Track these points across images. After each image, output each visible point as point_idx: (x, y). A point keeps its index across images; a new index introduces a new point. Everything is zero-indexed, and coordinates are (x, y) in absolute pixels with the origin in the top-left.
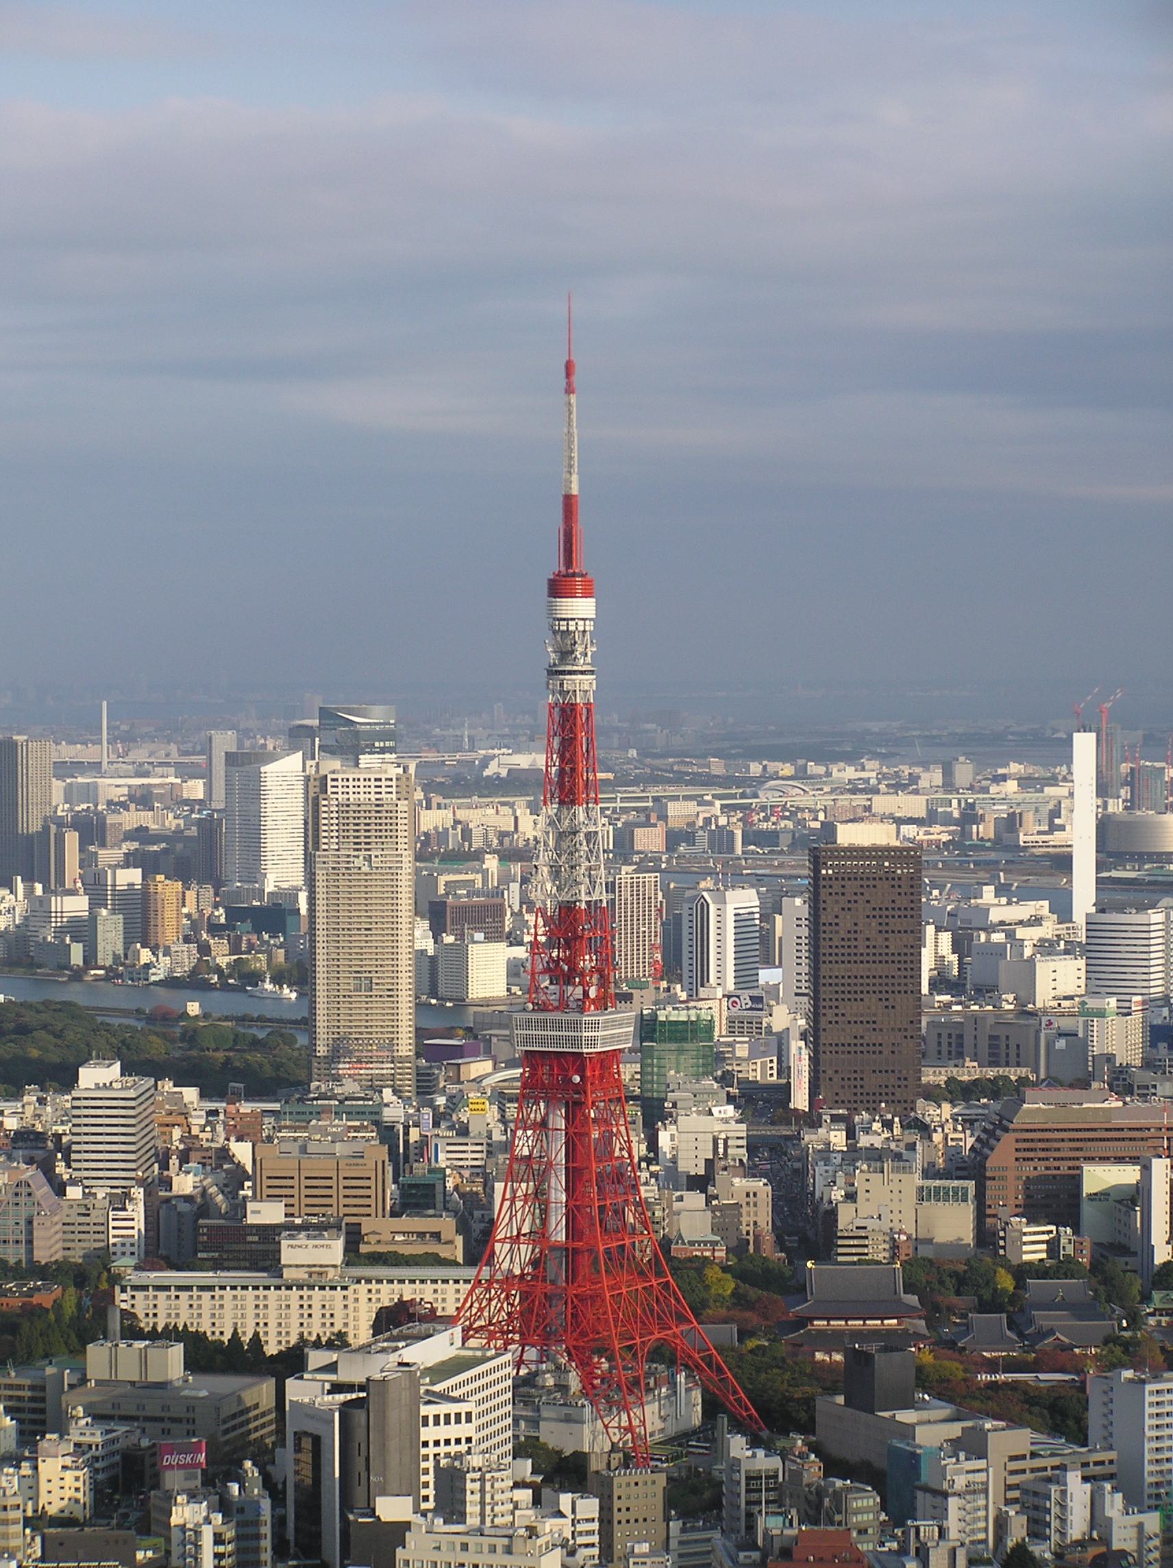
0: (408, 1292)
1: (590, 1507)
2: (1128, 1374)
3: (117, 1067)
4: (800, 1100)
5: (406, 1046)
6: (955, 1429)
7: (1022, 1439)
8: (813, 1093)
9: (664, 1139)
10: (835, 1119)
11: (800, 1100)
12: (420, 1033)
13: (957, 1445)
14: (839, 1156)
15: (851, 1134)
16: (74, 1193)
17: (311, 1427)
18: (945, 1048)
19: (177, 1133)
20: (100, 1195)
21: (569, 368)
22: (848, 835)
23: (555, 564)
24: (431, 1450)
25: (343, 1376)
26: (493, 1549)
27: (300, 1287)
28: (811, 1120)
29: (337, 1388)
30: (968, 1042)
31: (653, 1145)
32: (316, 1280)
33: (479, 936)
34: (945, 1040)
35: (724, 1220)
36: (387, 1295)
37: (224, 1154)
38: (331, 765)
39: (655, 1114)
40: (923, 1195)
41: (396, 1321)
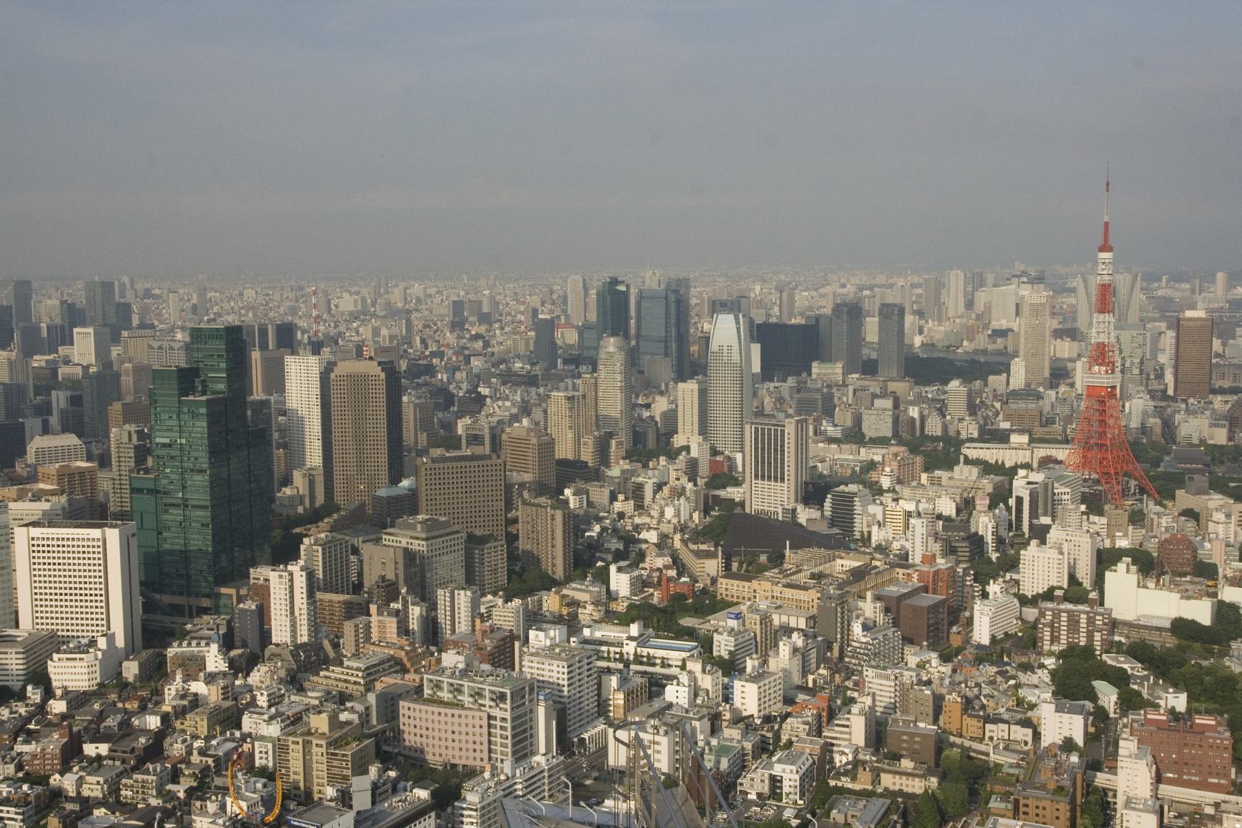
0: (1049, 452)
1: (1104, 520)
4: (1171, 392)
5: (1047, 374)
6: (1222, 502)
8: (1175, 390)
9: (1127, 405)
11: (1171, 392)
16: (948, 417)
17: (1020, 495)
21: (1108, 184)
22: (1189, 314)
23: (1100, 243)
25: (1031, 479)
28: (1174, 399)
31: (1123, 406)
32: (1020, 448)
40: (1212, 425)
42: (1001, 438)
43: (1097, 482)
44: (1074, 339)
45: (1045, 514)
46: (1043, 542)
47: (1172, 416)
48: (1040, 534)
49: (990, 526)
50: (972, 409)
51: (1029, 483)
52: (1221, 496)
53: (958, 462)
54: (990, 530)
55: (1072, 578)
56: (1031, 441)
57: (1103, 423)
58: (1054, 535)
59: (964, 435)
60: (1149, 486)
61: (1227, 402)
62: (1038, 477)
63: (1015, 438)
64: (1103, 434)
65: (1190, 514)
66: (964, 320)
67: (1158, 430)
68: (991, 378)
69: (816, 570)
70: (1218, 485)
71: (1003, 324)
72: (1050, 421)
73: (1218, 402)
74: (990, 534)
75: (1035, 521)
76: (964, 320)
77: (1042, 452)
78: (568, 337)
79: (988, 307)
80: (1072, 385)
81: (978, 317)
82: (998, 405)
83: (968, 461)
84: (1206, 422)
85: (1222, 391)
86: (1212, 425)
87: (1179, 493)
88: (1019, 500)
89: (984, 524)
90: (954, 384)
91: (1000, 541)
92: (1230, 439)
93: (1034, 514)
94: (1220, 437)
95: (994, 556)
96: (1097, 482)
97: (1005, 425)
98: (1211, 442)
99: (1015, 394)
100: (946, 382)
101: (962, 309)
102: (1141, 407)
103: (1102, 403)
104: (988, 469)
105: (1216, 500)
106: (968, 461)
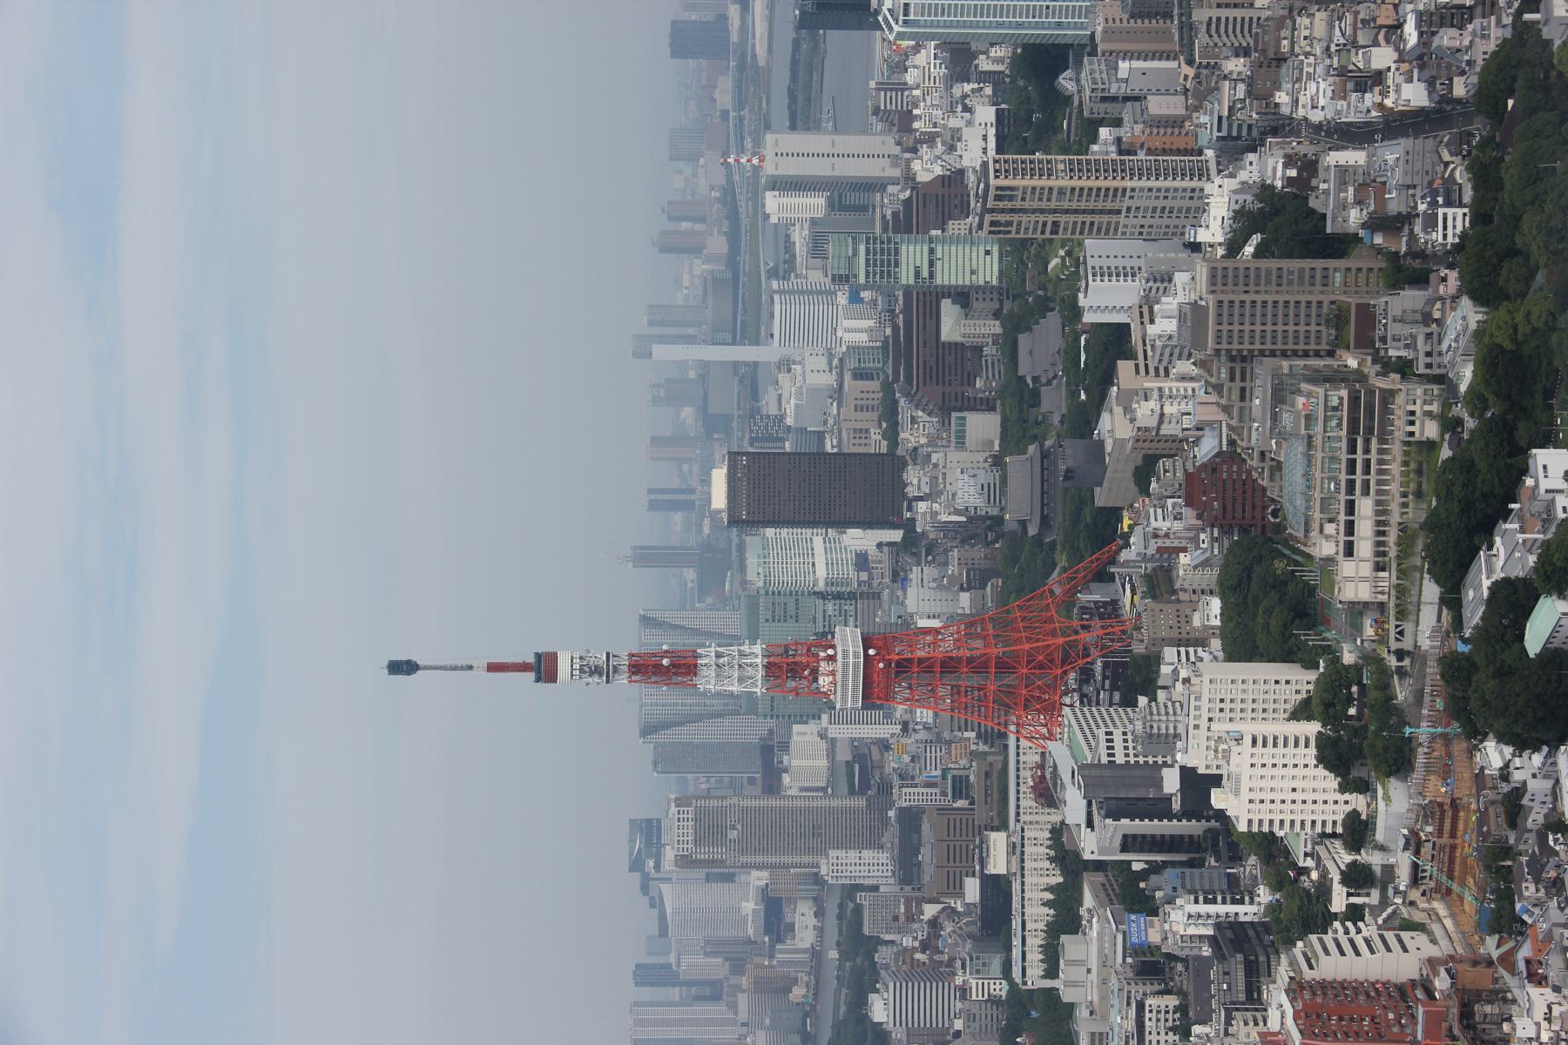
1: (1169, 653)
2: (1081, 296)
3: (872, 997)
5: (860, 802)
6: (1118, 410)
7: (1124, 368)
8: (894, 526)
10: (910, 509)
11: (896, 535)
12: (852, 792)
13: (1127, 410)
14: (935, 505)
15: (920, 499)
16: (958, 1024)
18: (863, 441)
19: (918, 956)
20: (959, 1005)
22: (719, 499)
24: (1132, 760)
25: (1082, 821)
26: (1197, 708)
27: (1023, 861)
29: (1090, 824)
30: (859, 425)
33: (785, 758)
34: (857, 441)
35: (975, 581)
36: (1028, 802)
37: (934, 923)
38: (669, 854)
39: (908, 631)
40: (961, 443)
42: (998, 891)
43: (1086, 675)
44: (785, 747)
45: (1159, 783)
46: (1216, 780)
47: (945, 527)
49: (1193, 909)
50: (939, 972)
51: (1090, 824)
52: (1105, 417)
53: (1052, 994)
54: (1203, 908)
55: (1301, 712)
56: (1003, 826)
57: (949, 665)
58: (1196, 756)
59: (1000, 989)
60: (1089, 562)
61: (914, 420)
62: (1074, 806)
63: (998, 864)
64: (978, 665)
65: (1144, 474)
66: (743, 1000)
67: (978, 553)
68: (866, 931)
70: (1083, 421)
71: (749, 906)
72: (960, 787)
73: (911, 437)
74: (1212, 909)
75: (1176, 805)
76: (743, 1000)
77: (1022, 799)
79: (713, 946)
80: (885, 745)
81: (738, 967)
82: (930, 910)
83: (1052, 972)
84: (954, 456)
85: (892, 435)
86: (961, 443)
87: (1102, 498)
88: (1129, 843)
89: (1186, 921)
90: (879, 1010)
91: (1236, 891)
92: (988, 406)
93: (1159, 808)
94: (983, 426)
95: (1264, 895)
96: (1086, 675)
97: (972, 889)
98: (997, 448)
99: (907, 869)
101: (718, 1010)
102: (926, 593)
103: (903, 667)
104: (1066, 920)
105: (1113, 426)
106: (1052, 972)
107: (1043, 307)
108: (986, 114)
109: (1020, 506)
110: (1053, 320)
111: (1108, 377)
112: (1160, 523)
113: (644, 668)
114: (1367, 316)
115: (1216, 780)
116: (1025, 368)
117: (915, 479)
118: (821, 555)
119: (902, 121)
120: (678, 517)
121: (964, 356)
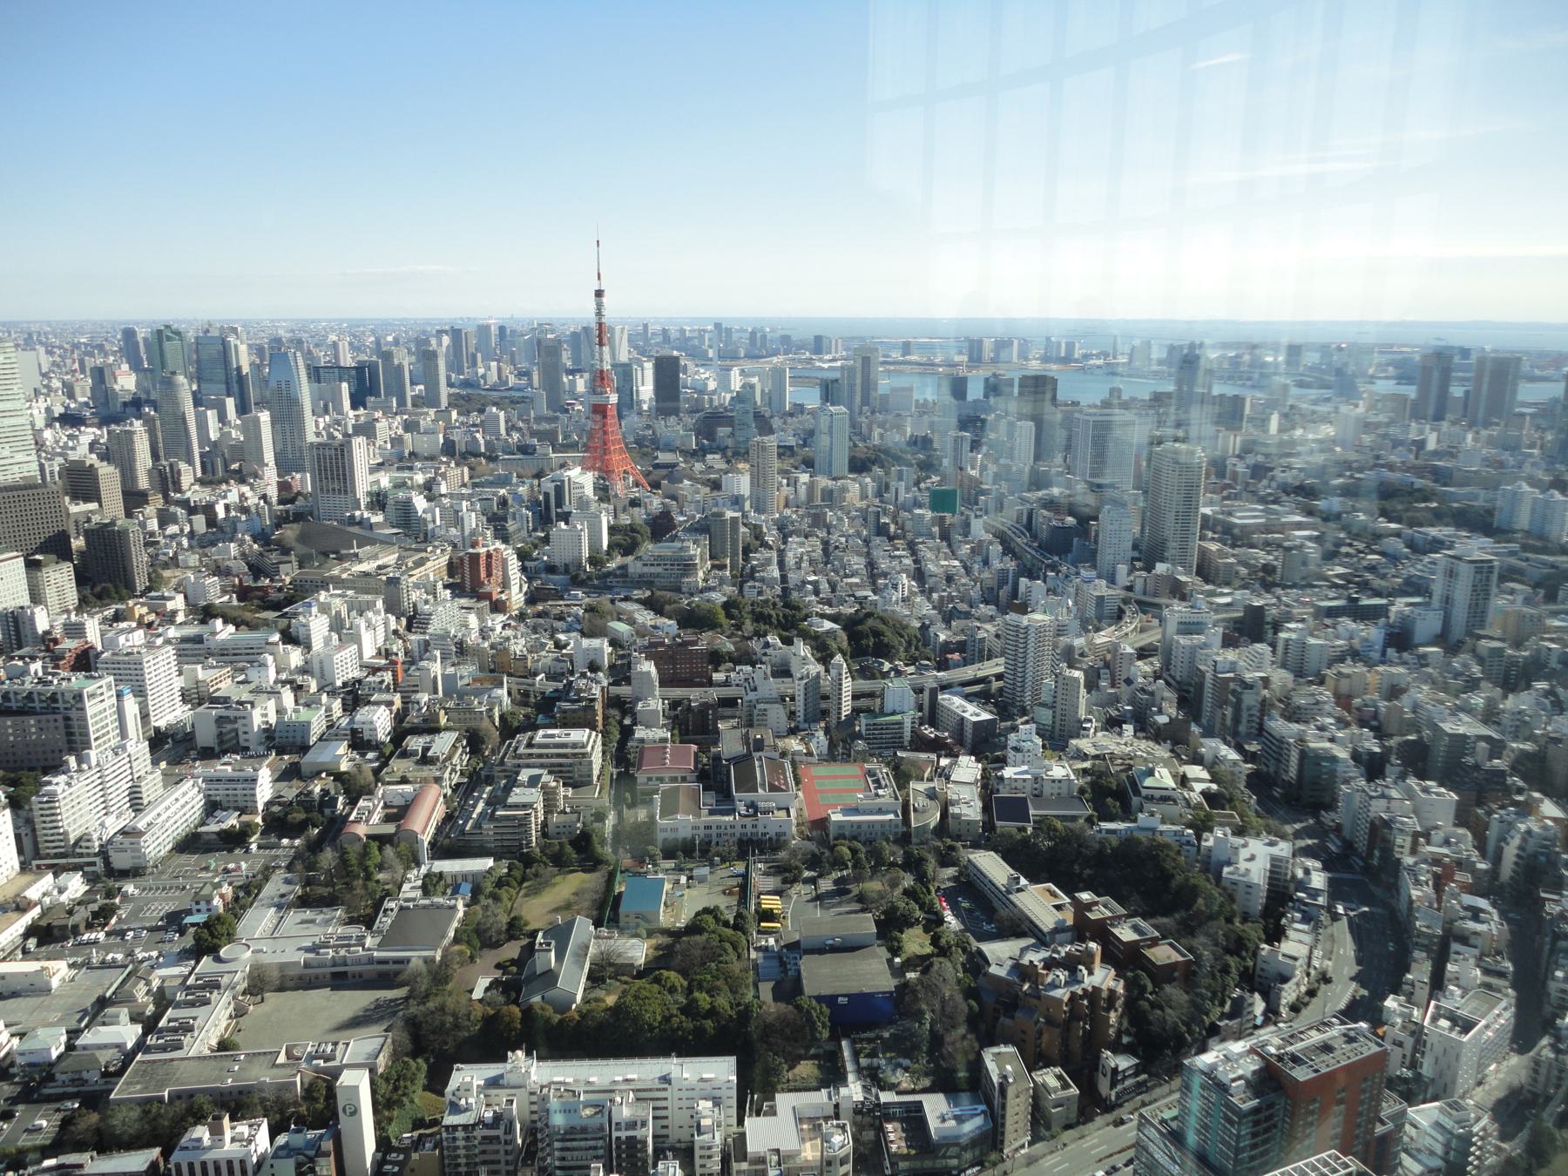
41: (563, 466)
48: (566, 517)
69: (380, 562)
78: (126, 382)
88: (547, 495)
99: (539, 419)
100: (481, 411)
103: (605, 417)
107: (728, 462)
108: (792, 441)
109: (664, 457)
110: (724, 466)
111: (703, 484)
112: (656, 503)
113: (600, 324)
114: (722, 567)
115: (567, 523)
116: (709, 456)
117: (673, 419)
118: (646, 390)
119: (791, 415)
120: (659, 339)
121: (711, 436)
